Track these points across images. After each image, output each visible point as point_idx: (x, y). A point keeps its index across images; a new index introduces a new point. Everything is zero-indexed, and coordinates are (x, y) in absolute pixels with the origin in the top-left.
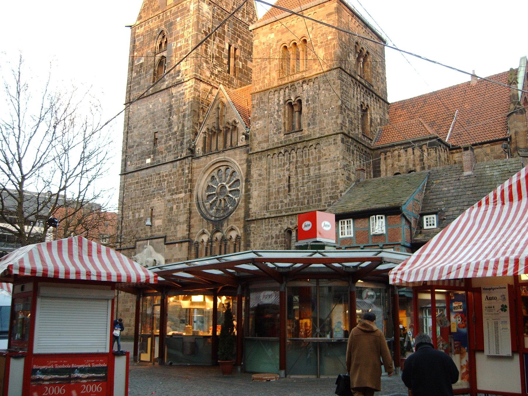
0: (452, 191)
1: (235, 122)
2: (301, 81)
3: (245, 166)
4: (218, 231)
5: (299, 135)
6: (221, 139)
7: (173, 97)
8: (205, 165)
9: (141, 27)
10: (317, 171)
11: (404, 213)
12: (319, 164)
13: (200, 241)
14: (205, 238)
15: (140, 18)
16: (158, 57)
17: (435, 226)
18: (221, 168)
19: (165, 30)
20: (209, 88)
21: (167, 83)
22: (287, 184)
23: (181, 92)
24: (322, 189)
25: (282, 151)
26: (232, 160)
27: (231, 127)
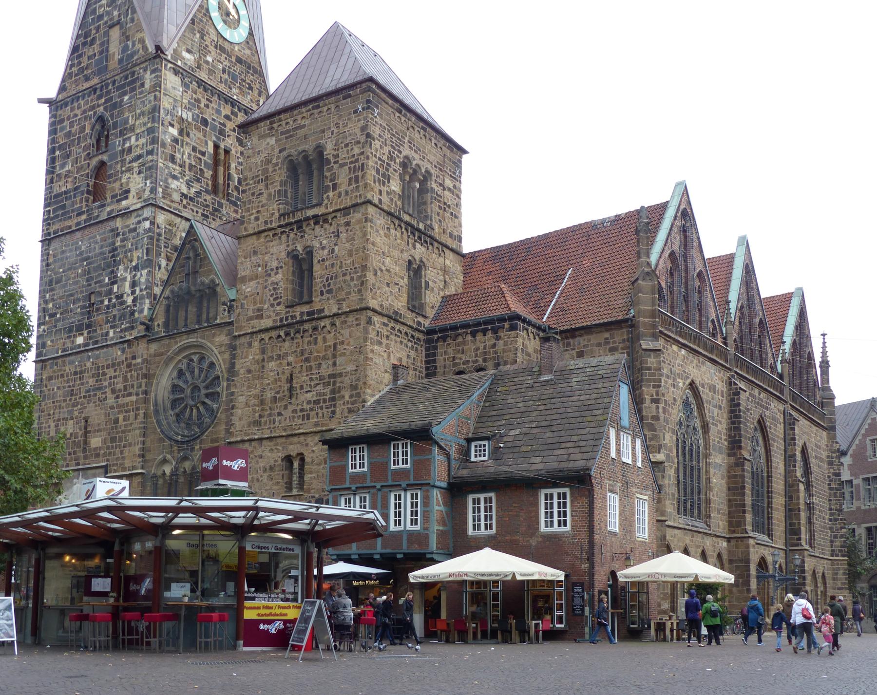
0: (520, 405)
1: (213, 281)
2: (312, 222)
3: (227, 356)
4: (185, 458)
5: (306, 309)
6: (192, 309)
7: (118, 235)
8: (168, 351)
9: (66, 105)
10: (331, 369)
11: (437, 437)
12: (334, 356)
13: (159, 473)
14: (168, 469)
15: (62, 89)
16: (94, 162)
17: (486, 458)
18: (193, 357)
19: (107, 115)
21: (108, 209)
22: (286, 387)
23: (132, 227)
24: (337, 395)
25: (282, 334)
26: (209, 344)
27: (207, 291)
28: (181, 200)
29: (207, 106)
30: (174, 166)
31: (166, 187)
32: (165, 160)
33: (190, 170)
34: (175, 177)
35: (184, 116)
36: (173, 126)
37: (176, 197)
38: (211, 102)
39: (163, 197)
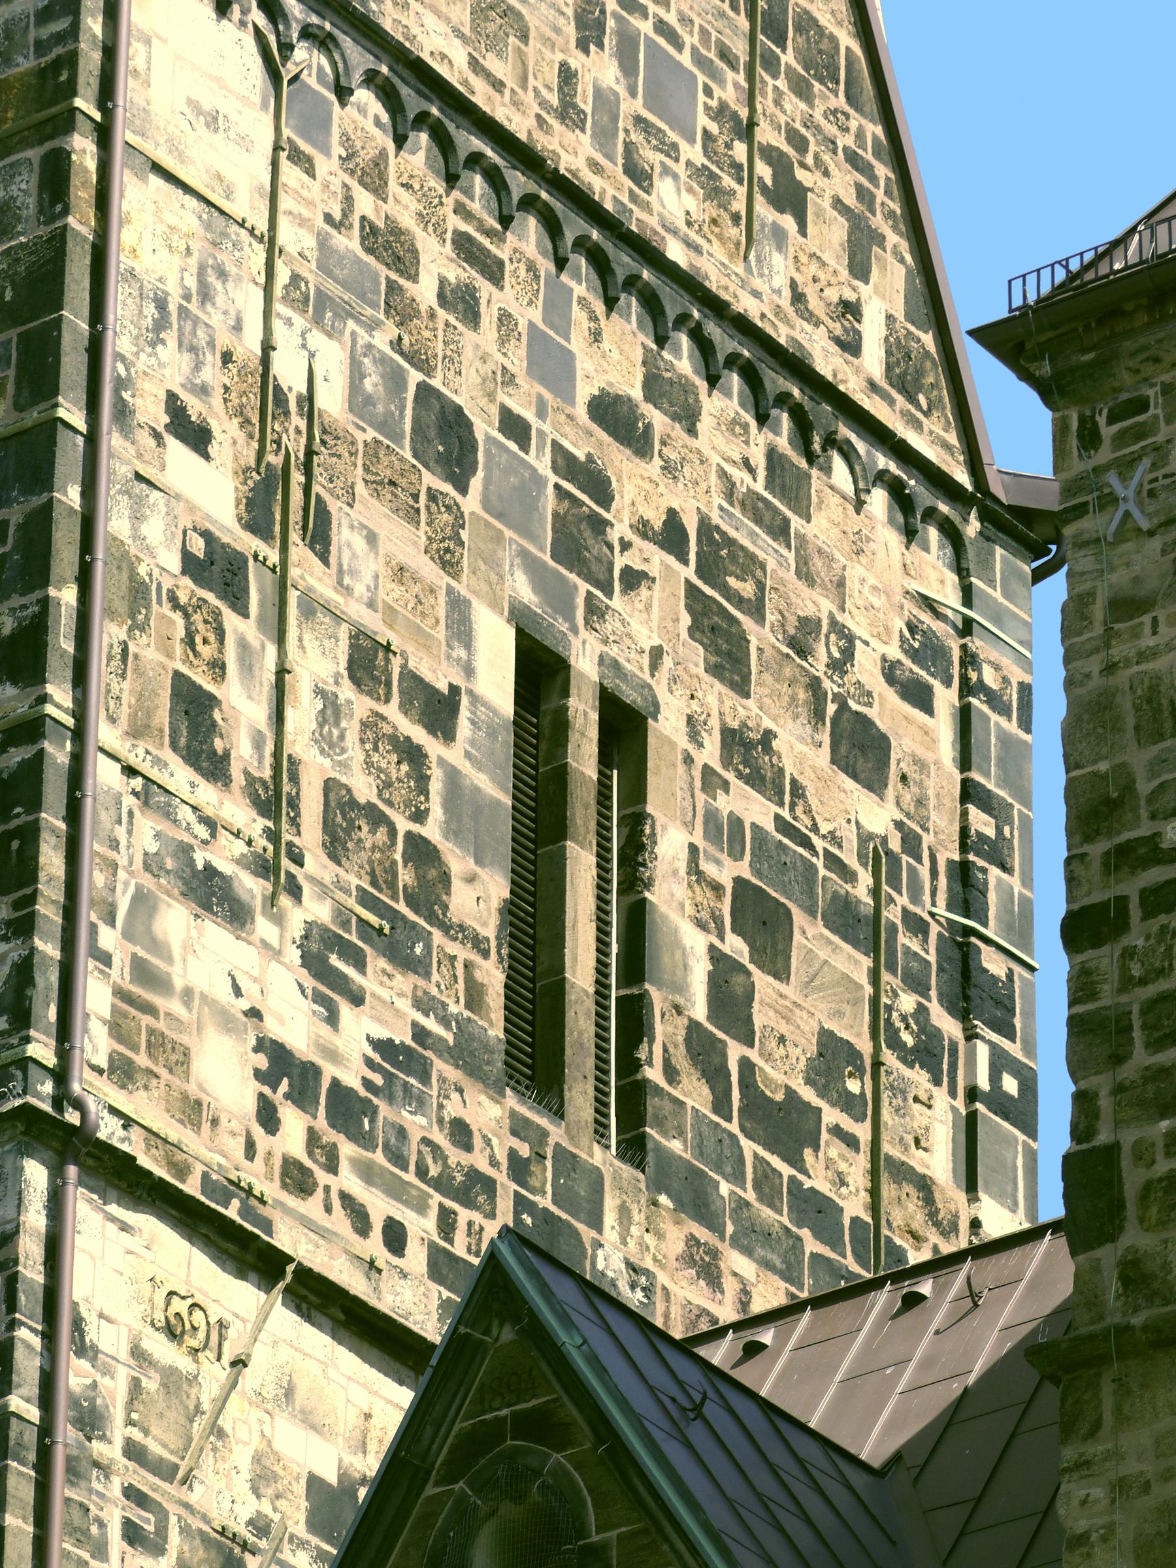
20: (234, 1297)
28: (268, 1118)
29: (462, 303)
30: (207, 794)
31: (142, 971)
32: (136, 732)
33: (335, 847)
34: (210, 893)
35: (289, 372)
36: (198, 438)
37: (226, 1075)
38: (494, 272)
39: (122, 1071)
